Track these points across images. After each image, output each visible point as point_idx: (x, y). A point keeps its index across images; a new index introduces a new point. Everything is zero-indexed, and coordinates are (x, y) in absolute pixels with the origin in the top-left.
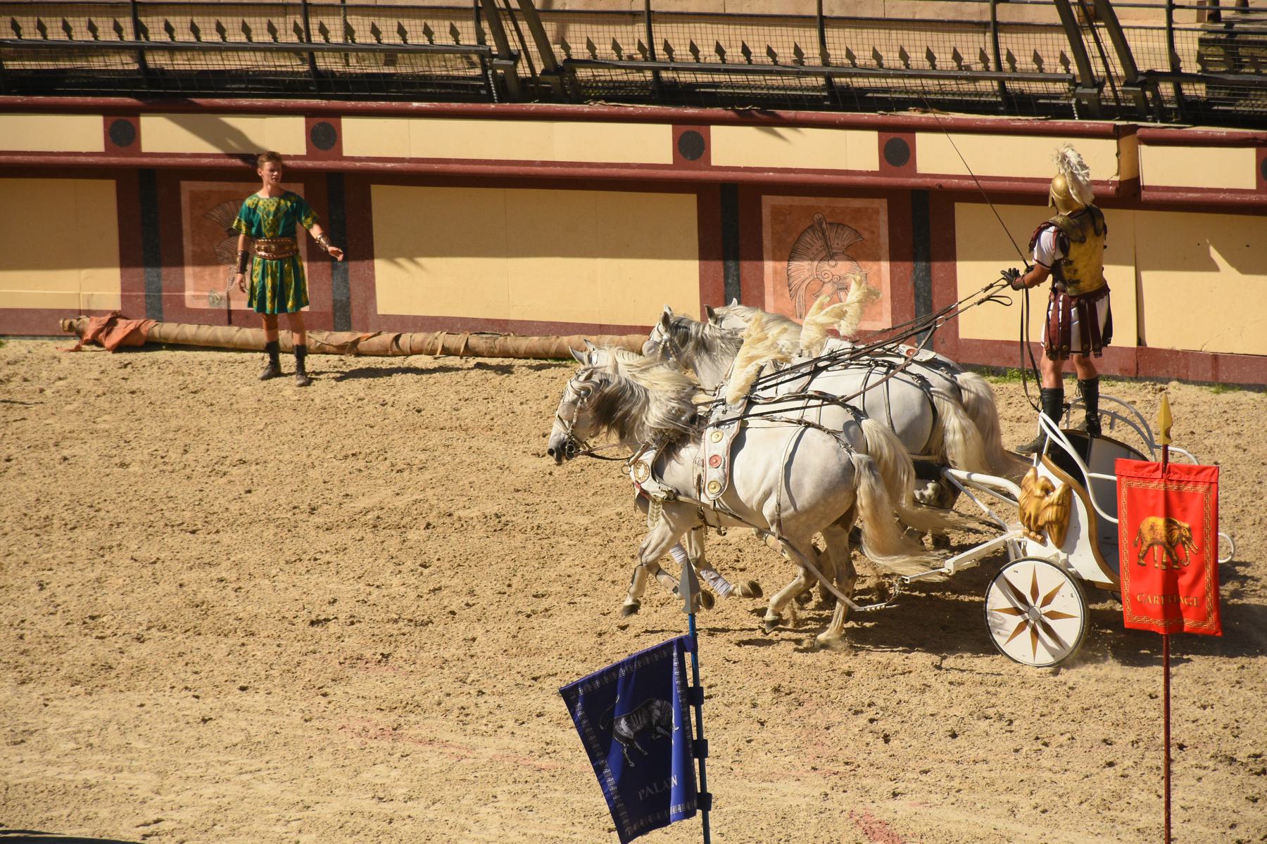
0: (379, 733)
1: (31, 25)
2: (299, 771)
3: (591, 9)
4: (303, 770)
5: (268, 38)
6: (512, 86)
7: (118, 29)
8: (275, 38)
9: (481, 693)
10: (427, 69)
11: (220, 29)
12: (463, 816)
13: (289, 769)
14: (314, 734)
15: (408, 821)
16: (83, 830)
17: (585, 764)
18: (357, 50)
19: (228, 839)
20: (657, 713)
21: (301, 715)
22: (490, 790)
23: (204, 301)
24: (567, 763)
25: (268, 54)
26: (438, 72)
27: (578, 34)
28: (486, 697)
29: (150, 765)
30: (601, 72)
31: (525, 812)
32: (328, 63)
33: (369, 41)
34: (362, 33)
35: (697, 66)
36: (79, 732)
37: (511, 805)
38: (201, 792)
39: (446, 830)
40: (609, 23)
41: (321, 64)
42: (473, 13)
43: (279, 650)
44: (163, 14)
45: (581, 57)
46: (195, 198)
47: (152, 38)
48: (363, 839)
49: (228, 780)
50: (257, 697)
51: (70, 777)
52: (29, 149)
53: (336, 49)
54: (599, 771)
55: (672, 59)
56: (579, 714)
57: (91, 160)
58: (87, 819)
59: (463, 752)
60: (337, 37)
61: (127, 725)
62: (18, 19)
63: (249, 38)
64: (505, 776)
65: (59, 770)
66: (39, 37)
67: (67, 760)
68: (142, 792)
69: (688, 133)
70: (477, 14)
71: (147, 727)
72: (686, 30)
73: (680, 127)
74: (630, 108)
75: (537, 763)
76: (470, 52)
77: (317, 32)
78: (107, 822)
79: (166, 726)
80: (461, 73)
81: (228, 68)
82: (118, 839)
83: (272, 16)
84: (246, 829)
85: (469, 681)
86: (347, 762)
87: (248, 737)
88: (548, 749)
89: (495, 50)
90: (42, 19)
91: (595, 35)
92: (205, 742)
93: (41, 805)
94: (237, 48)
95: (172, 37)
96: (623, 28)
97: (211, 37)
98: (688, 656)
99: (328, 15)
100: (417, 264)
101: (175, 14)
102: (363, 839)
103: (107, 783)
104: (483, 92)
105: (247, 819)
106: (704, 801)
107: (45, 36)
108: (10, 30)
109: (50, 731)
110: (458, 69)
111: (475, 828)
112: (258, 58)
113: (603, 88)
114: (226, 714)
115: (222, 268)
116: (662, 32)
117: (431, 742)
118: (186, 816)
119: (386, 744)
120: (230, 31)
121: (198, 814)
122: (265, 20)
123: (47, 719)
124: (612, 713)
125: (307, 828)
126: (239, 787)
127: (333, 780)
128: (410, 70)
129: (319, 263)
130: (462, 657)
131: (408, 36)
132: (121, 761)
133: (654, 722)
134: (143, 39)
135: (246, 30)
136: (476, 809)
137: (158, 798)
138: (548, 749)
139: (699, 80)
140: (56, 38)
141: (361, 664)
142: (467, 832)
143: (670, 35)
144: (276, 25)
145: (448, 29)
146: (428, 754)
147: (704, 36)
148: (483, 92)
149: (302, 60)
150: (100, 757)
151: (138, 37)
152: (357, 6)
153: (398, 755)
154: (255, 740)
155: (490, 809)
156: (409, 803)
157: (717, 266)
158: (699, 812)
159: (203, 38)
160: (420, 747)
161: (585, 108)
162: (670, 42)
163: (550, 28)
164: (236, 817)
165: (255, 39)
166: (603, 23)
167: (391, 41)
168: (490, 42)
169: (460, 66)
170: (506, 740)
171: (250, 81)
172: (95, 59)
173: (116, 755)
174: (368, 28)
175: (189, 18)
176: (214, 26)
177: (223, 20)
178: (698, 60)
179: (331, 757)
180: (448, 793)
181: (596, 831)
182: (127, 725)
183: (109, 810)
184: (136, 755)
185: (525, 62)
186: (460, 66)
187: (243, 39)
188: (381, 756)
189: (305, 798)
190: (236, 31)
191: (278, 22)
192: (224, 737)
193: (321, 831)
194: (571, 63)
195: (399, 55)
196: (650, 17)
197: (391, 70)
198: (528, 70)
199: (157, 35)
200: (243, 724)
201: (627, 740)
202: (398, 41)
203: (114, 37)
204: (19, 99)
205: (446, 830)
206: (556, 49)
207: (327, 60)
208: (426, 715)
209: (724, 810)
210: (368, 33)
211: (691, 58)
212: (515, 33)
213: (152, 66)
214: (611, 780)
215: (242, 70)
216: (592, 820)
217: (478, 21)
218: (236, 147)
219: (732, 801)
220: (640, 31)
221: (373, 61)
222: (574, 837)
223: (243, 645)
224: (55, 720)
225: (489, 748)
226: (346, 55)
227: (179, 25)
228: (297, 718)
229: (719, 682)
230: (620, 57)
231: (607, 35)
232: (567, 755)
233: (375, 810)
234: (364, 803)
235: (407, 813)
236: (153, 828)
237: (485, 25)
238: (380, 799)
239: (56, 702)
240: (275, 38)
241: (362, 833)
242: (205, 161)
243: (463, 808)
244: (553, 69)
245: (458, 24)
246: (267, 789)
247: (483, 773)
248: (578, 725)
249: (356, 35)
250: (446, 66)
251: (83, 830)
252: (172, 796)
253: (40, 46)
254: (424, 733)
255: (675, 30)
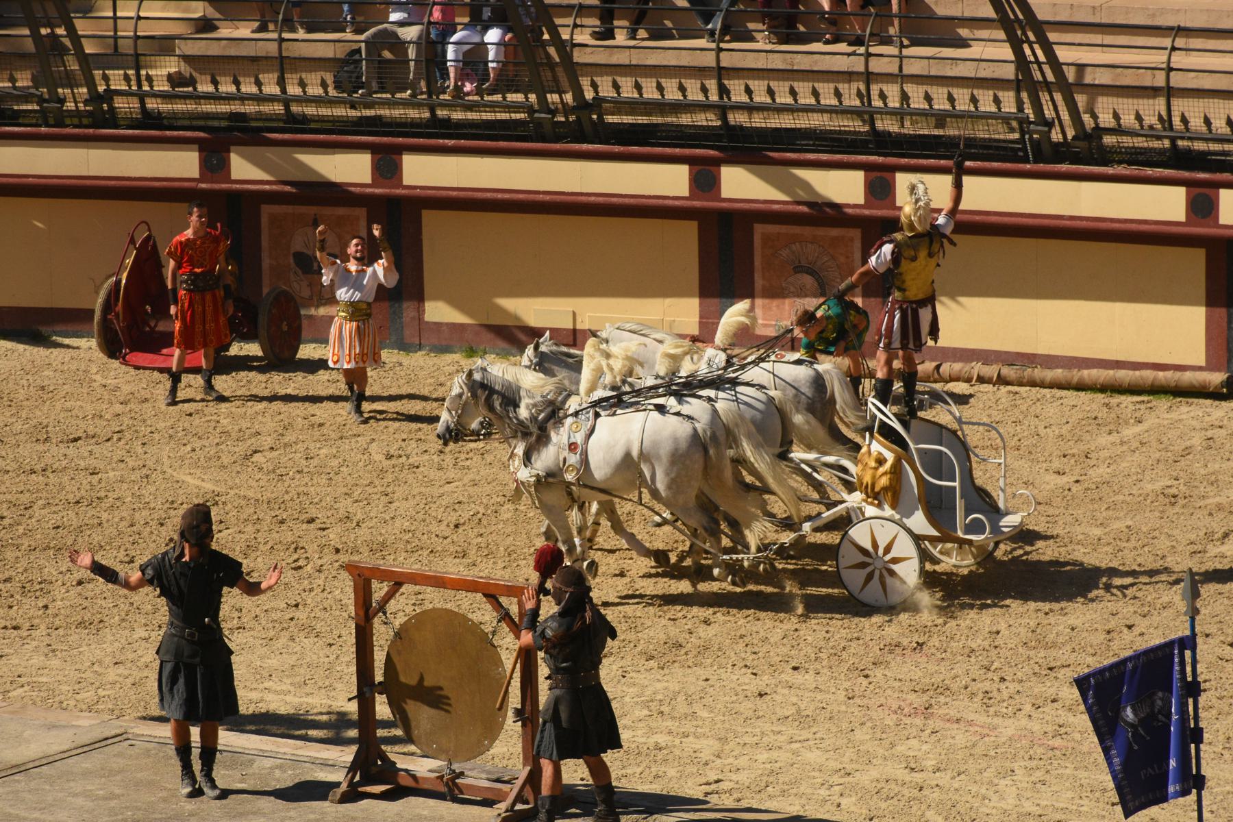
0: (912, 711)
1: (629, 84)
2: (842, 742)
3: (1118, 84)
4: (845, 741)
5: (834, 102)
6: (1046, 148)
7: (704, 90)
8: (841, 103)
9: (1003, 679)
10: (972, 132)
11: (793, 93)
12: (984, 787)
13: (833, 740)
14: (856, 710)
15: (936, 789)
16: (654, 786)
17: (1093, 745)
18: (911, 114)
19: (779, 799)
20: (1159, 703)
21: (845, 693)
22: (1008, 764)
23: (771, 329)
24: (1076, 744)
25: (834, 115)
26: (981, 135)
27: (1105, 106)
28: (1007, 684)
29: (713, 732)
30: (1125, 139)
31: (1039, 785)
32: (886, 125)
33: (922, 106)
34: (916, 100)
35: (1210, 136)
36: (652, 701)
37: (1027, 779)
38: (756, 758)
39: (969, 798)
40: (1133, 97)
41: (880, 125)
42: (1014, 86)
43: (828, 636)
44: (743, 78)
45: (1107, 125)
46: (766, 239)
47: (733, 99)
48: (896, 803)
49: (780, 748)
50: (807, 677)
51: (643, 740)
52: (624, 193)
53: (893, 113)
54: (1106, 751)
55: (1187, 130)
56: (1090, 701)
57: (677, 203)
58: (656, 776)
59: (986, 731)
60: (894, 103)
61: (694, 697)
62: (618, 79)
63: (818, 101)
64: (1022, 753)
65: (634, 733)
66: (636, 95)
67: (641, 725)
68: (705, 755)
69: (1199, 195)
70: (1017, 85)
71: (711, 699)
72: (1201, 104)
73: (1192, 189)
74: (1149, 171)
75: (1049, 743)
76: (1010, 118)
77: (877, 97)
78: (674, 780)
79: (727, 698)
80: (1002, 137)
81: (798, 126)
82: (683, 795)
83: (838, 82)
84: (794, 791)
85: (993, 668)
86: (884, 736)
87: (799, 711)
88: (1060, 731)
89: (1032, 117)
90: (639, 80)
91: (1121, 106)
92: (761, 714)
93: (618, 763)
94: (807, 109)
95: (751, 99)
96: (1146, 101)
97: (784, 99)
98: (1188, 653)
99: (887, 83)
100: (958, 303)
101: (754, 78)
102: (896, 803)
103: (675, 746)
104: (1021, 154)
105: (796, 782)
106: (1194, 782)
107: (641, 94)
108: (611, 89)
109: (627, 699)
110: (999, 133)
111: (995, 798)
112: (825, 119)
113: (1126, 153)
114: (779, 690)
115: (787, 301)
116: (1179, 105)
117: (958, 721)
118: (742, 777)
119: (918, 721)
120: (802, 95)
121: (753, 776)
122: (832, 86)
123: (625, 688)
124: (1119, 702)
125: (847, 792)
126: (789, 755)
127: (871, 750)
128: (957, 133)
129: (873, 299)
130: (987, 647)
131: (956, 103)
132: (688, 727)
133: (1156, 710)
134: (726, 100)
135: (815, 93)
136: (996, 781)
137: (719, 761)
138: (1060, 731)
139: (1211, 148)
140: (650, 96)
141: (899, 650)
142: (987, 801)
143: (1186, 108)
144: (841, 91)
145: (991, 98)
146: (955, 732)
147: (1217, 110)
148: (1021, 154)
149: (864, 121)
150: (669, 723)
151: (721, 97)
152: (913, 76)
153: (929, 731)
154: (805, 713)
155: (1008, 781)
156: (937, 774)
157: (1222, 312)
158: (1194, 791)
159: (778, 100)
160: (948, 725)
161: (1110, 170)
162: (1186, 114)
163: (1081, 100)
164: (786, 780)
165: (822, 102)
166: (1128, 96)
167: (942, 107)
168: (1028, 110)
169: (1001, 130)
170: (1024, 722)
171: (817, 139)
172: (683, 116)
173: (683, 722)
174: (922, 95)
175: (766, 82)
176: (787, 89)
177: (795, 85)
178: (1210, 130)
179: (870, 731)
180: (971, 766)
181: (1101, 805)
182: (694, 697)
183: (676, 769)
184: (701, 723)
185: (1058, 128)
186: (1001, 130)
187: (813, 101)
188: (914, 732)
189: (847, 766)
190: (807, 95)
191: (843, 87)
192: (778, 709)
193: (860, 795)
194: (1099, 131)
195: (948, 119)
196: (1170, 92)
197: (941, 132)
198: (1060, 136)
199: (738, 96)
200: (794, 700)
201: (1132, 725)
202: (948, 107)
203: (701, 97)
204: (617, 149)
205: (969, 798)
206: (1086, 118)
207: (885, 122)
208: (954, 697)
209: (1214, 791)
210: (922, 100)
211: (1204, 129)
212: (1050, 103)
213: (733, 123)
214: (1116, 760)
215: (810, 128)
216: (1098, 794)
217: (1018, 92)
218: (803, 195)
219: (1222, 783)
220: (1160, 104)
221: (925, 124)
222: (1081, 809)
223: (796, 630)
224: (631, 690)
225: (1009, 728)
226: (902, 119)
227: (757, 88)
228: (841, 695)
229: (1213, 677)
230: (1142, 126)
231: (1131, 107)
232: (1077, 736)
233: (907, 779)
234: (898, 772)
235: (935, 783)
236: (714, 787)
237: (1024, 95)
238: (912, 769)
239: (632, 674)
240: (841, 103)
241: (895, 799)
242: (776, 207)
243: (985, 780)
244: (1082, 134)
245: (1000, 94)
246: (813, 757)
247: (1003, 750)
248: (1089, 710)
249: (911, 101)
250: (988, 130)
251: (654, 786)
252: (731, 760)
253: (637, 103)
254: (952, 713)
255: (1191, 104)
